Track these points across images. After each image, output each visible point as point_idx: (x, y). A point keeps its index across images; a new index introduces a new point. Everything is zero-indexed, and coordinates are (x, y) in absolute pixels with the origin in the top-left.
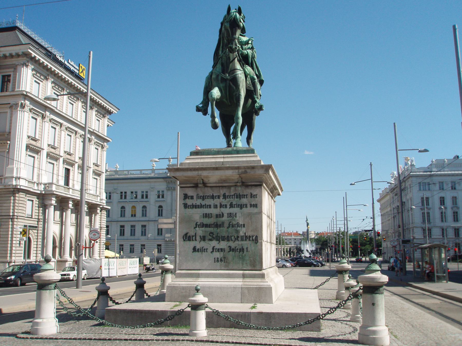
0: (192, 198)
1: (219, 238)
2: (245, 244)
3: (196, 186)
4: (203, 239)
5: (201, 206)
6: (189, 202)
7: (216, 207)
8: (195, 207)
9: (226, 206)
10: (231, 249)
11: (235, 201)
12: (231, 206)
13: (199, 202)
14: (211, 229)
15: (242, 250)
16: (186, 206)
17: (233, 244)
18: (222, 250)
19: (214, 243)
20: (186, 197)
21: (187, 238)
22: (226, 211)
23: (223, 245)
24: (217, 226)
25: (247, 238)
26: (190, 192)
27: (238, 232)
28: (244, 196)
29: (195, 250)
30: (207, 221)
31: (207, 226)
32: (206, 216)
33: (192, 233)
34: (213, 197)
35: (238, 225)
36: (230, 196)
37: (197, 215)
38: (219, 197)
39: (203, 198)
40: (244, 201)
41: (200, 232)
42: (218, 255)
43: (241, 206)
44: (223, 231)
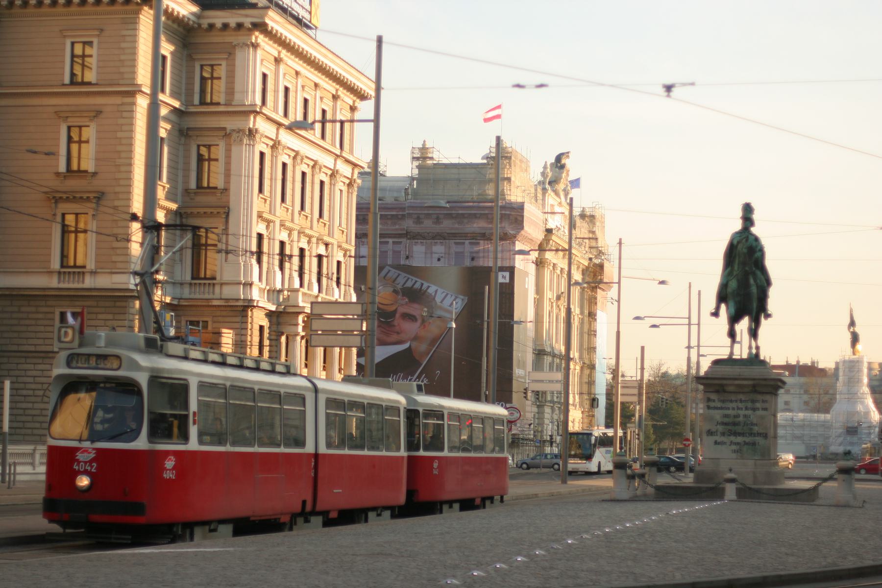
0: (714, 401)
1: (736, 434)
2: (758, 439)
3: (717, 392)
4: (723, 434)
5: (721, 408)
6: (712, 404)
7: (733, 409)
8: (716, 408)
9: (742, 409)
10: (746, 443)
11: (749, 405)
12: (746, 409)
13: (719, 405)
14: (730, 427)
15: (754, 444)
16: (709, 407)
17: (748, 439)
18: (738, 444)
19: (733, 438)
20: (709, 400)
21: (710, 433)
22: (742, 413)
23: (739, 439)
24: (734, 424)
25: (759, 434)
26: (713, 396)
27: (751, 429)
28: (757, 401)
29: (716, 443)
30: (726, 420)
31: (726, 424)
32: (726, 416)
33: (714, 429)
34: (731, 401)
35: (752, 424)
36: (745, 401)
37: (717, 415)
38: (736, 401)
39: (723, 401)
40: (758, 405)
41: (720, 428)
42: (734, 447)
43: (754, 409)
44: (739, 429)
